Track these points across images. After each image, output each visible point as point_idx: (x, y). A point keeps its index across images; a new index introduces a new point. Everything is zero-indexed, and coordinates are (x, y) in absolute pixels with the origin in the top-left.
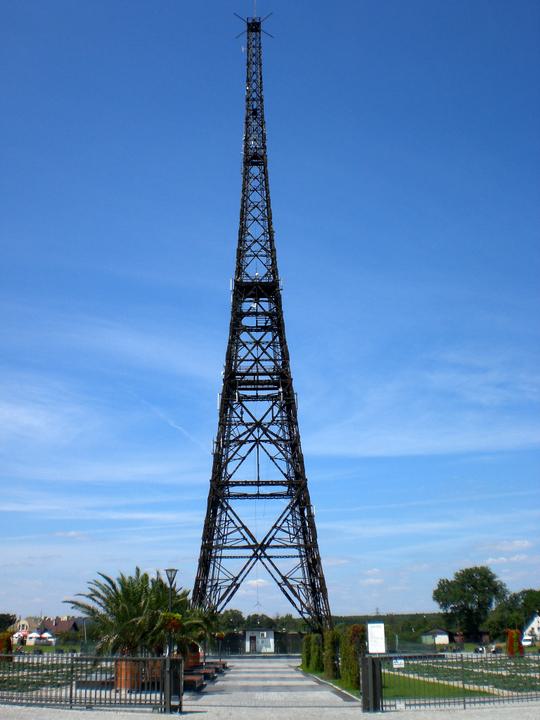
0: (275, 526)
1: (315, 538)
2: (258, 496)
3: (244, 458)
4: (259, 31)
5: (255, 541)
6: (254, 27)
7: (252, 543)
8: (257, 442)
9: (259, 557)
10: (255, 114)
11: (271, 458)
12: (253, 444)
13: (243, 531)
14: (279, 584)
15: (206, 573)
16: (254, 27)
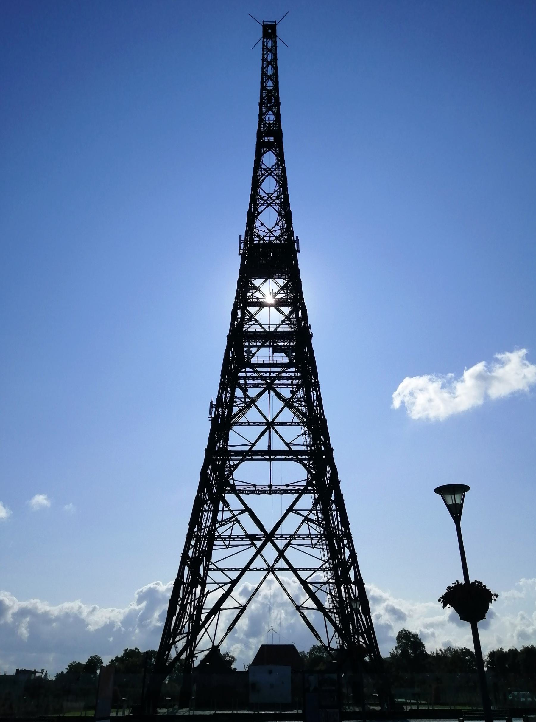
0: (290, 509)
1: (345, 523)
2: (271, 490)
3: (254, 445)
4: (275, 37)
5: (261, 526)
6: (270, 31)
7: (256, 531)
8: (270, 425)
9: (271, 569)
10: (270, 99)
11: (287, 445)
12: (264, 427)
13: (245, 518)
14: (298, 608)
15: (199, 580)
16: (270, 31)
